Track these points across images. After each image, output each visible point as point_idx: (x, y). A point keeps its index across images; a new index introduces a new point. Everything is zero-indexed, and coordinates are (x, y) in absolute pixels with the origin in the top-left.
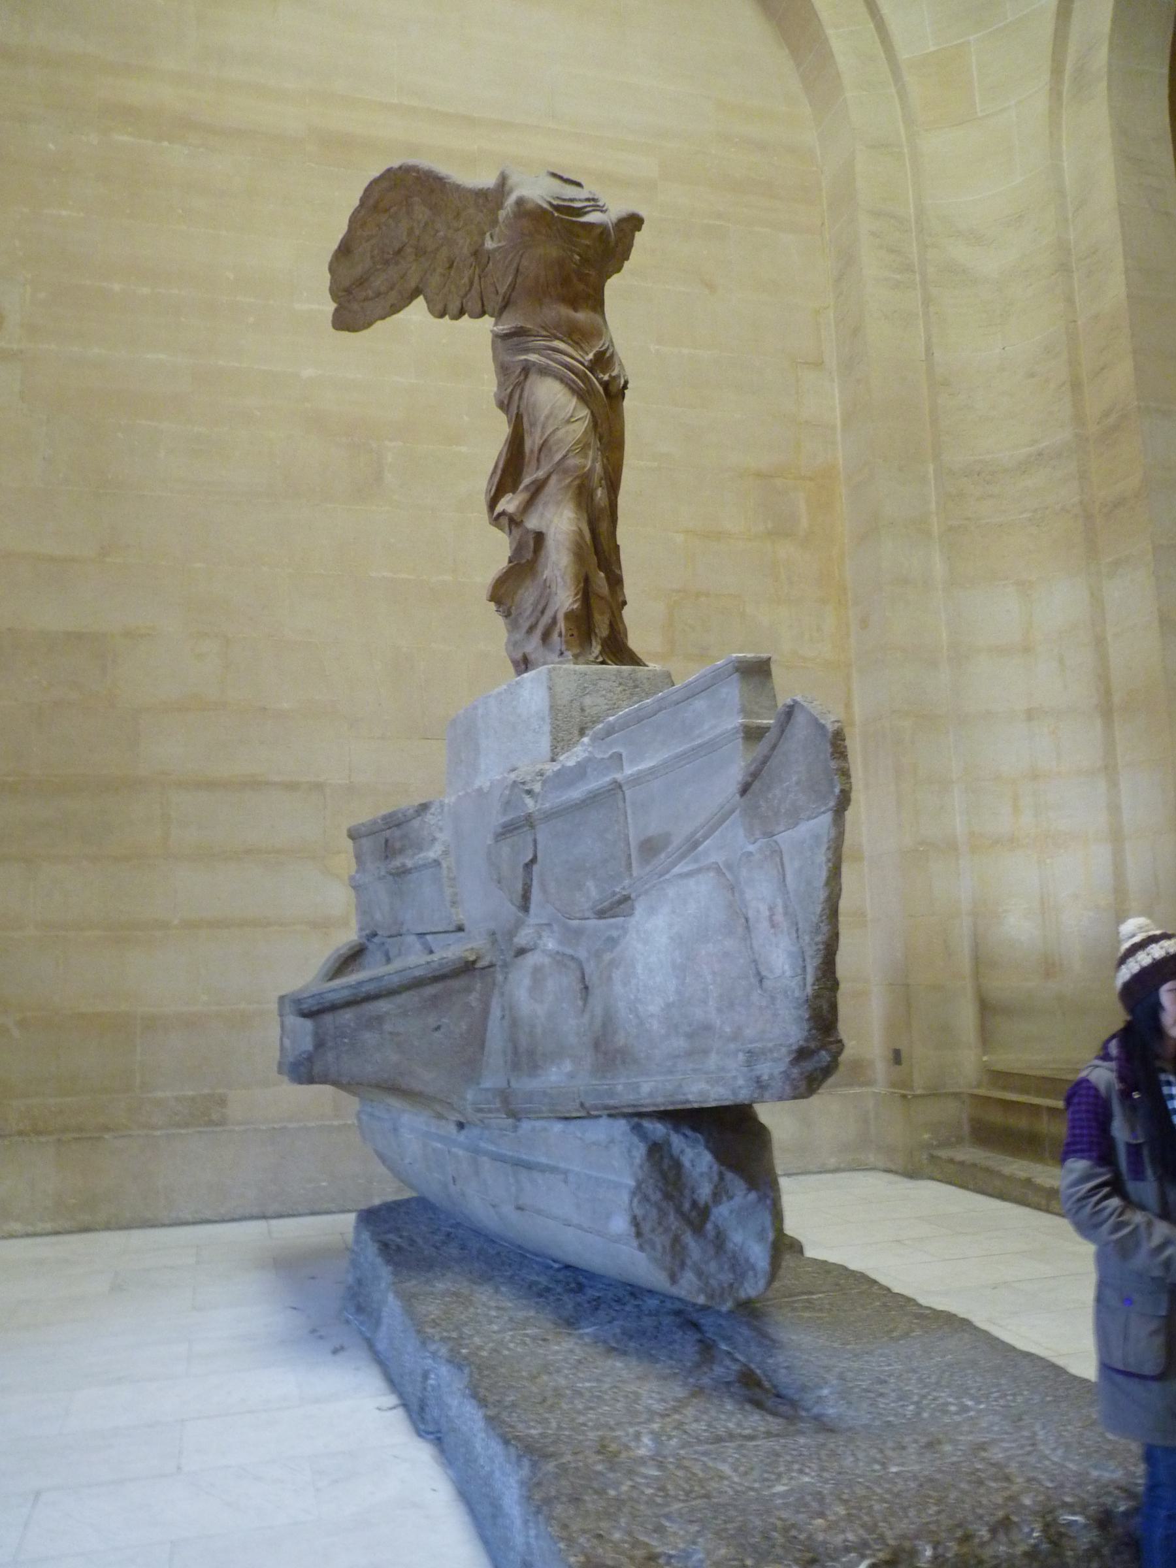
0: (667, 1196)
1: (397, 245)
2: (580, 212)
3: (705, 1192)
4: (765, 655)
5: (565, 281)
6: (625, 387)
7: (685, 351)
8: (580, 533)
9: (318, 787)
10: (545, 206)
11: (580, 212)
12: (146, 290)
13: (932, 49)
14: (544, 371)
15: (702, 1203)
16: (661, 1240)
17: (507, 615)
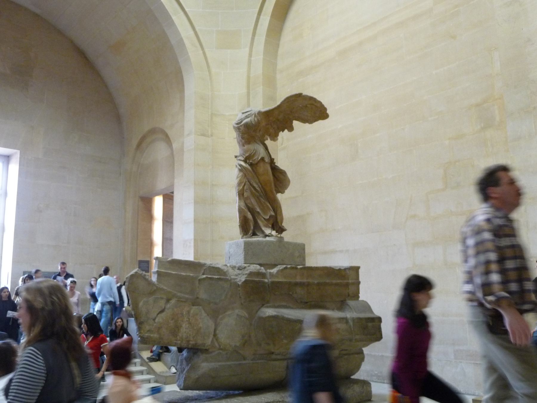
8: (239, 206)
9: (347, 251)
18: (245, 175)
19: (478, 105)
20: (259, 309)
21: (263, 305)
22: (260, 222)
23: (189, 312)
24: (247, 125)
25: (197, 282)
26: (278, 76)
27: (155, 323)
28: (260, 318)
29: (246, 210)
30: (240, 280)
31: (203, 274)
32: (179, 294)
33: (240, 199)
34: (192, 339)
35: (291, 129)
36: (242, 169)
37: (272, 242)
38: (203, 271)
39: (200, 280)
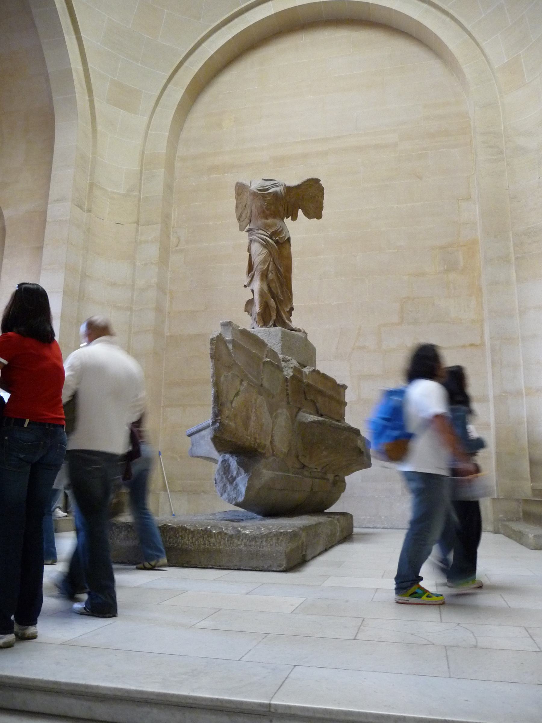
0: (225, 474)
1: (245, 204)
2: (267, 190)
3: (235, 473)
4: (229, 321)
5: (263, 212)
6: (289, 239)
7: (409, 205)
10: (256, 191)
11: (267, 190)
12: (220, 222)
13: (507, 61)
14: (255, 241)
15: (234, 476)
16: (221, 485)
17: (251, 316)
18: (270, 254)
19: (441, 248)
20: (297, 413)
21: (300, 409)
22: (283, 313)
23: (256, 400)
24: (275, 194)
25: (262, 365)
26: (178, 164)
27: (232, 407)
28: (301, 424)
29: (269, 295)
30: (288, 374)
31: (266, 357)
32: (249, 376)
33: (262, 279)
34: (257, 437)
35: (294, 217)
36: (266, 245)
37: (301, 338)
38: (266, 353)
39: (264, 363)
